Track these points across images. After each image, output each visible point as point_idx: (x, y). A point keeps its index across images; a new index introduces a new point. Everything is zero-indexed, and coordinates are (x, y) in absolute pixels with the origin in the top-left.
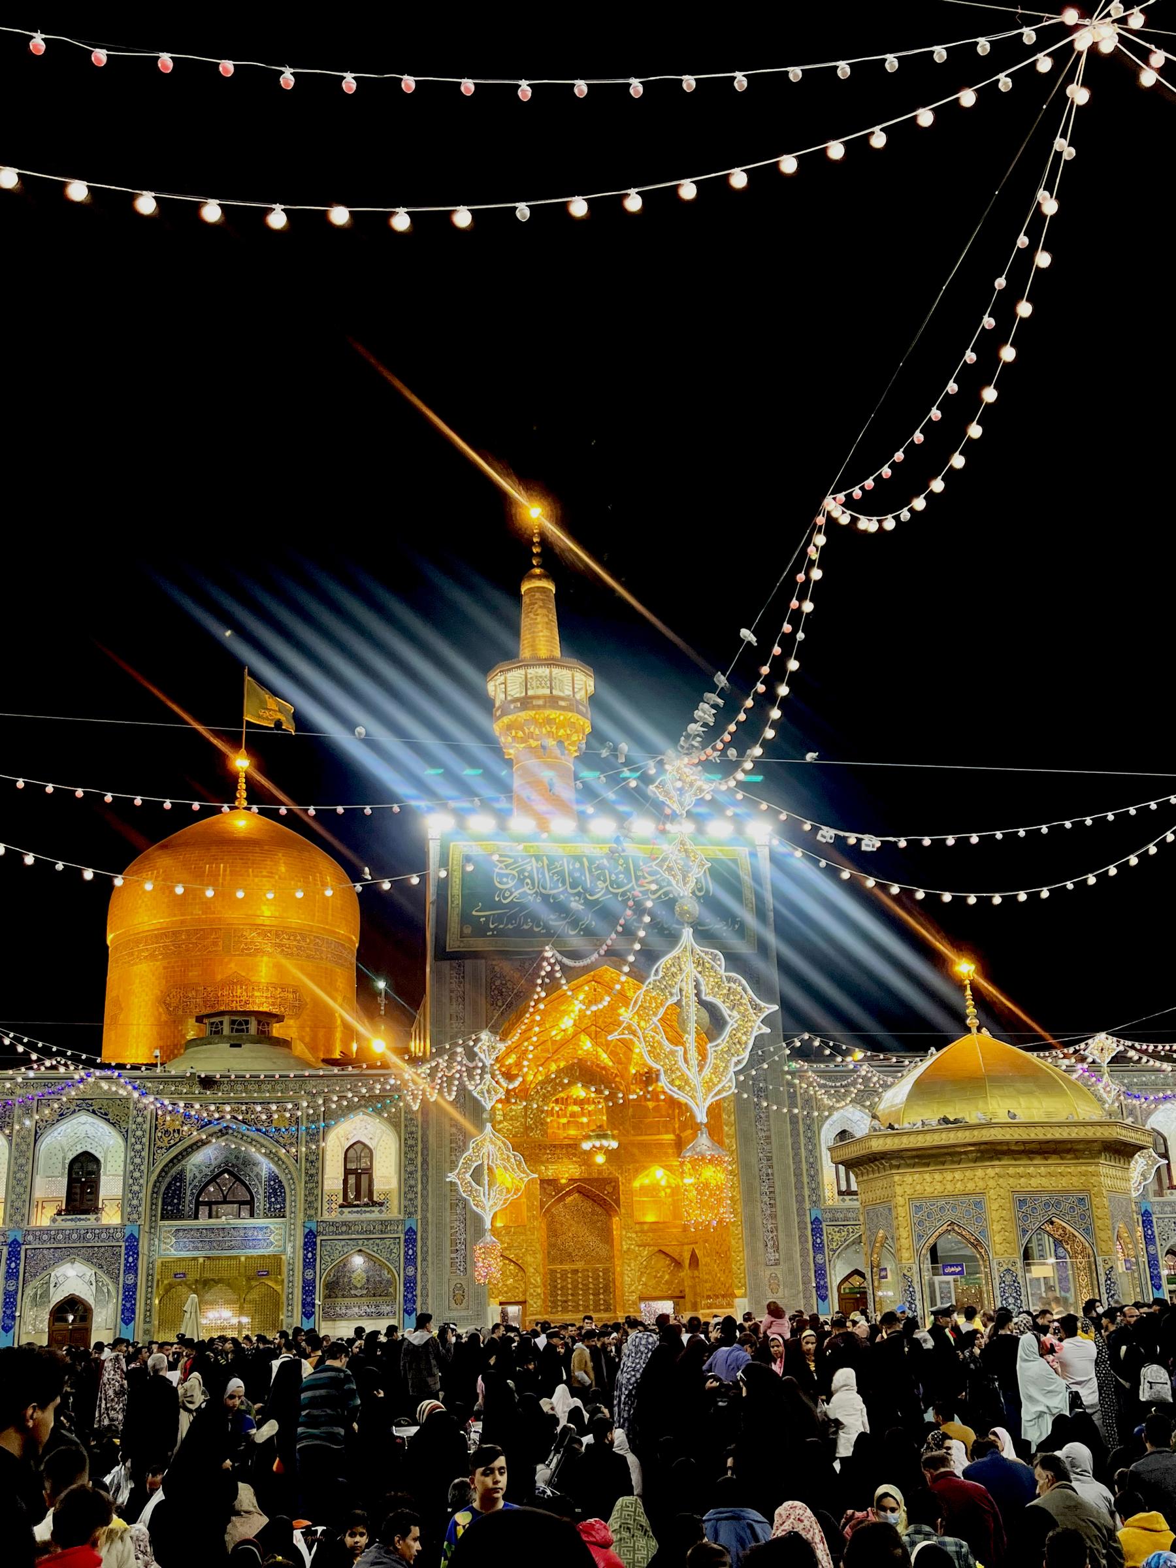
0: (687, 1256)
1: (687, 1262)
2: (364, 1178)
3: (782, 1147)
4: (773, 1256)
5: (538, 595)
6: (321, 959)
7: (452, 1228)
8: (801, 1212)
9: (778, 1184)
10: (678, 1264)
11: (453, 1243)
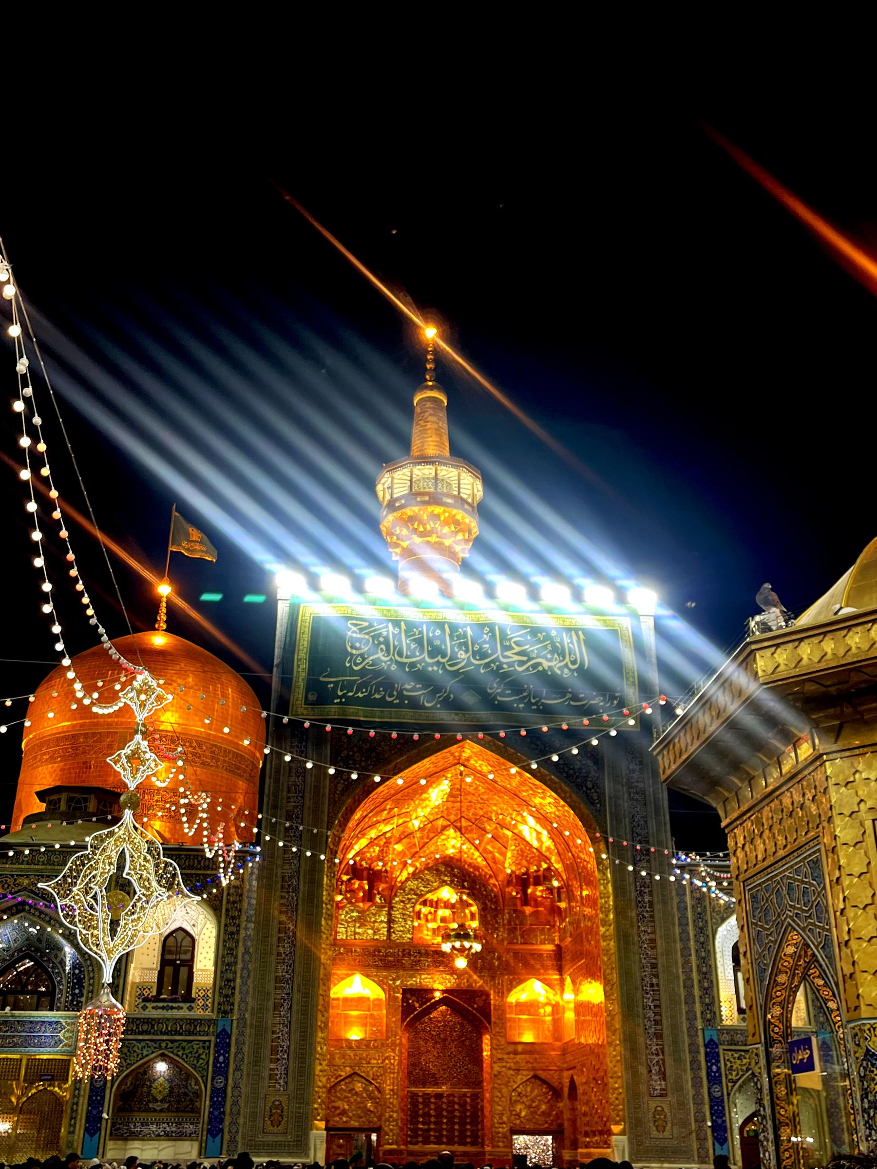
0: (566, 1082)
1: (566, 1090)
2: (184, 971)
3: (668, 953)
4: (659, 1085)
5: (429, 404)
6: (217, 767)
7: (274, 1032)
8: (692, 1031)
9: (664, 998)
10: (557, 1093)
11: (274, 1050)
